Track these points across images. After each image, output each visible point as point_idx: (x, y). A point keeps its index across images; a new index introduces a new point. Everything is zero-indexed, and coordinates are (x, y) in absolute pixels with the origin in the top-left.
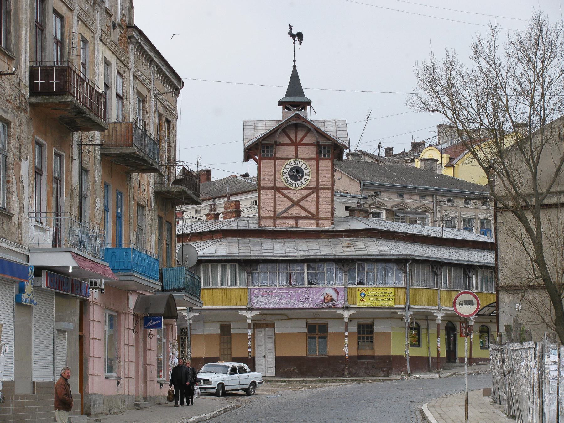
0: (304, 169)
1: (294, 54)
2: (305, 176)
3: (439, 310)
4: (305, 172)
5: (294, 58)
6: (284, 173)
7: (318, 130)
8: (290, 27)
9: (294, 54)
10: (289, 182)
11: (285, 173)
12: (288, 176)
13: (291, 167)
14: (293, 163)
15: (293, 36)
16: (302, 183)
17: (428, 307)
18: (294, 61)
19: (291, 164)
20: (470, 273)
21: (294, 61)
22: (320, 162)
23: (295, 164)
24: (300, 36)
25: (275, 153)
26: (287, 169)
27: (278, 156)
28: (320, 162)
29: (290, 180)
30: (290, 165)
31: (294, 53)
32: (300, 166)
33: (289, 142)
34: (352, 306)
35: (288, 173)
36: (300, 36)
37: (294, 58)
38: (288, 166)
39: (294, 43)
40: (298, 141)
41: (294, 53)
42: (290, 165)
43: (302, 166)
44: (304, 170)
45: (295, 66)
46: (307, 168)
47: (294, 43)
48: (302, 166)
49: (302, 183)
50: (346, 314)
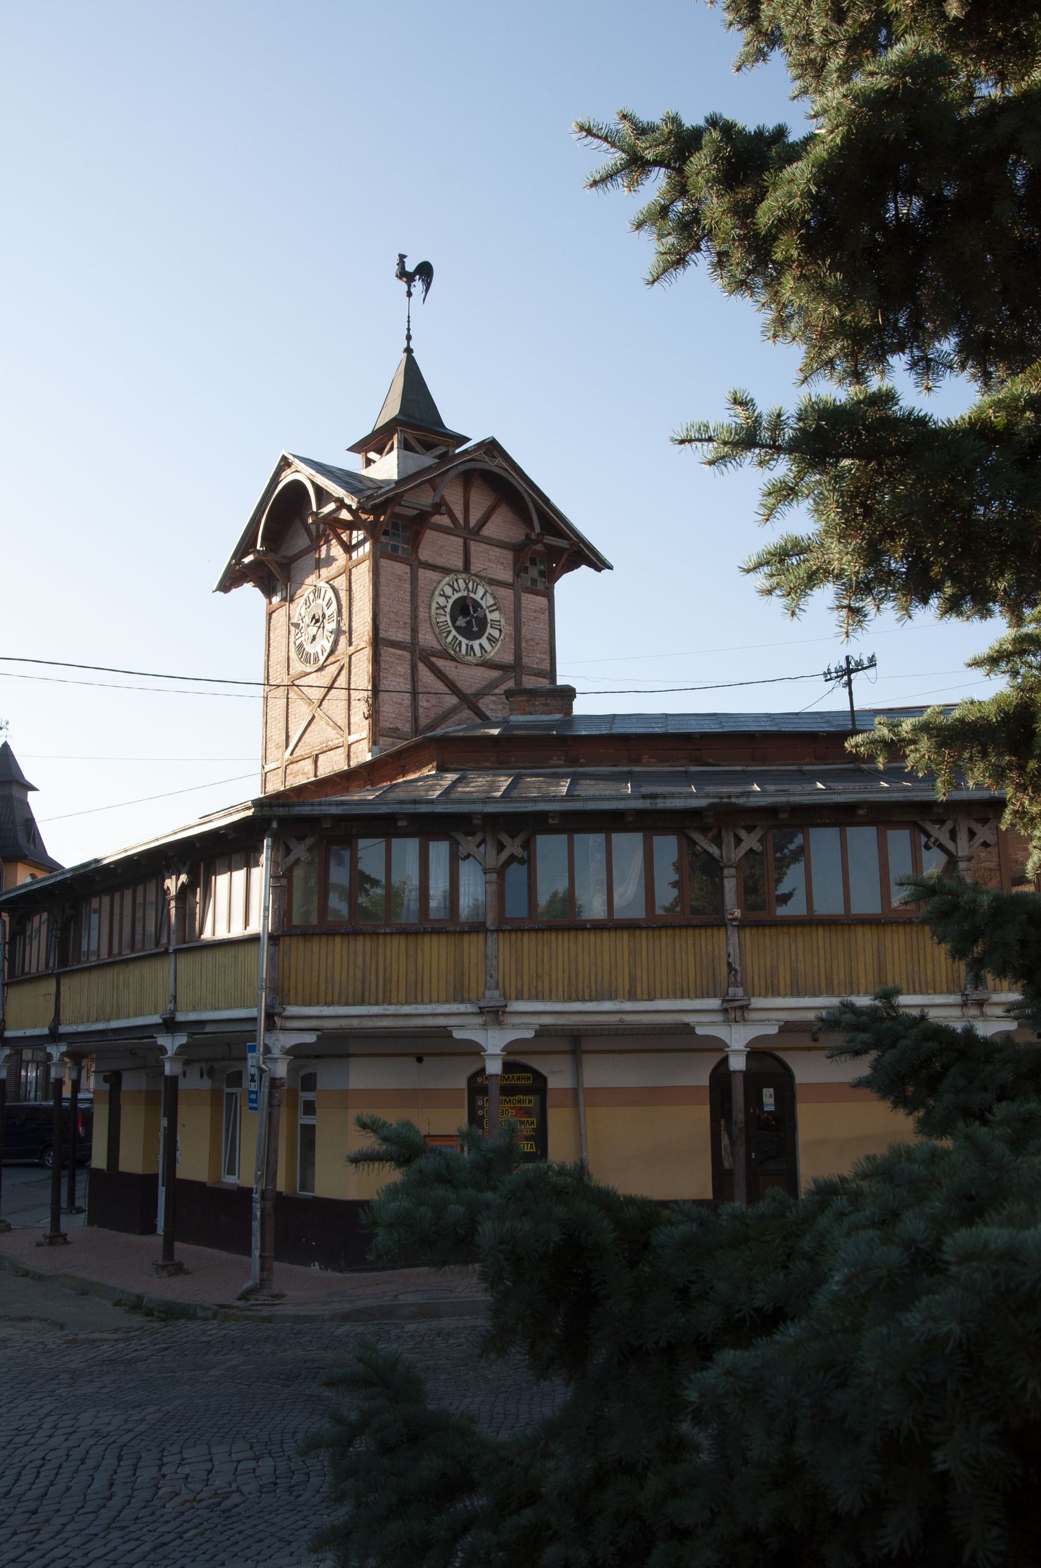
1: (409, 321)
3: (494, 1015)
5: (409, 329)
8: (402, 257)
9: (409, 321)
15: (403, 274)
17: (406, 1009)
18: (409, 338)
20: (720, 846)
21: (409, 338)
24: (425, 271)
31: (409, 317)
34: (180, 1017)
36: (425, 271)
37: (409, 329)
39: (409, 294)
41: (409, 317)
45: (409, 351)
47: (409, 294)
50: (171, 1043)
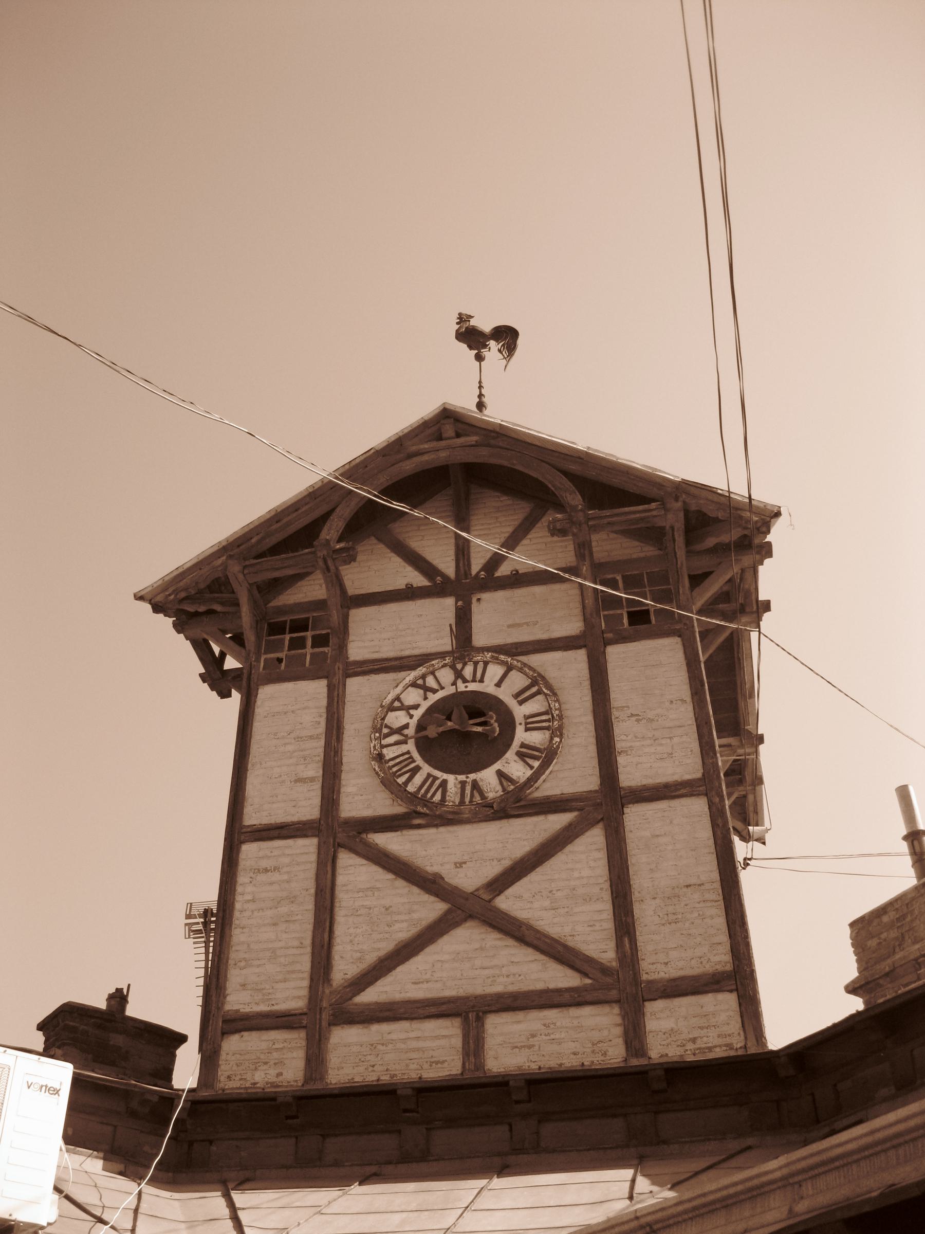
0: (516, 696)
2: (521, 736)
4: (520, 712)
6: (387, 736)
7: (573, 468)
10: (418, 779)
11: (399, 730)
12: (411, 746)
13: (433, 698)
14: (446, 676)
16: (501, 774)
19: (431, 682)
22: (616, 654)
23: (459, 675)
25: (342, 647)
26: (408, 709)
27: (357, 651)
28: (616, 654)
29: (426, 769)
30: (427, 689)
32: (488, 687)
33: (419, 580)
35: (411, 731)
38: (412, 696)
40: (476, 567)
42: (427, 689)
43: (498, 685)
44: (512, 703)
46: (534, 689)
48: (498, 685)
49: (501, 774)
